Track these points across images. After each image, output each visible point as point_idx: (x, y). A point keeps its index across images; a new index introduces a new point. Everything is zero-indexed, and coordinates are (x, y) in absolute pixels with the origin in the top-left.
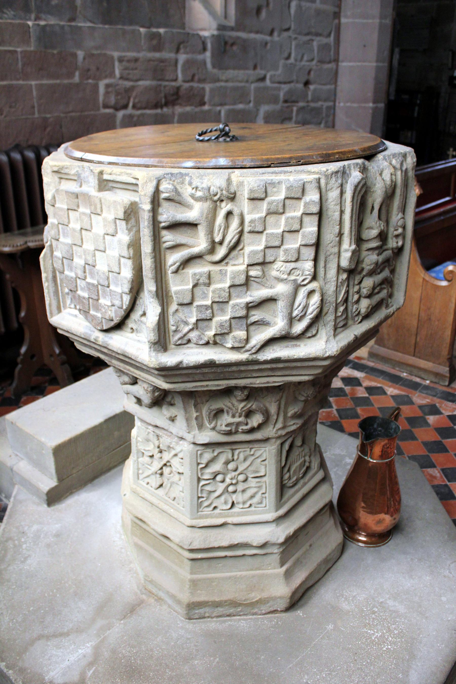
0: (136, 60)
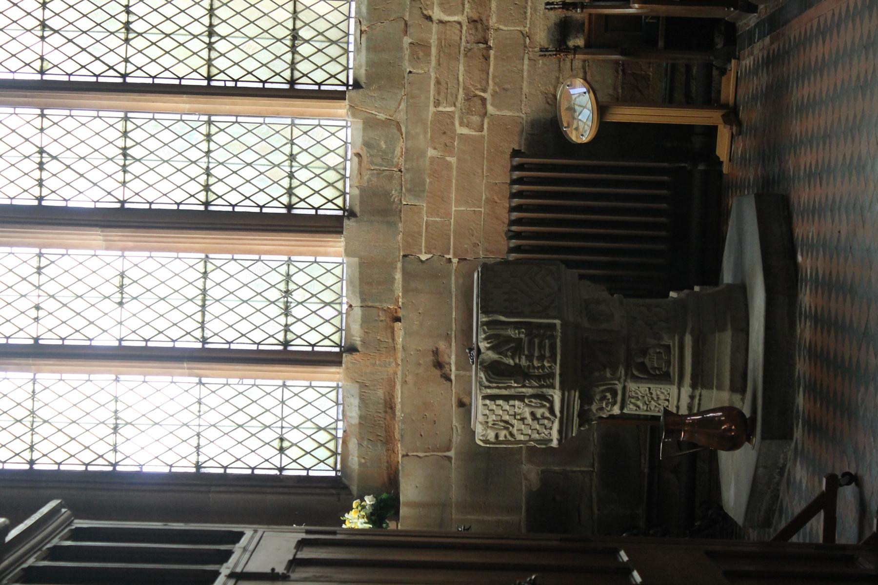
0: (438, 82)
